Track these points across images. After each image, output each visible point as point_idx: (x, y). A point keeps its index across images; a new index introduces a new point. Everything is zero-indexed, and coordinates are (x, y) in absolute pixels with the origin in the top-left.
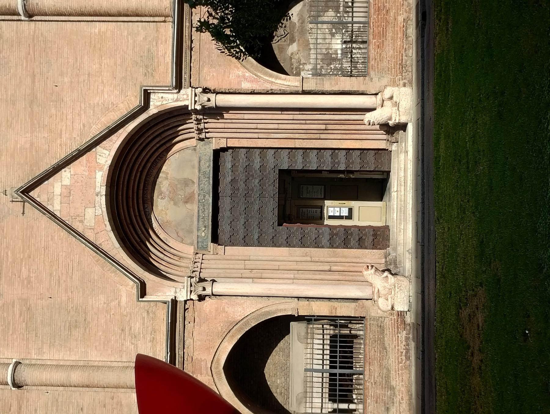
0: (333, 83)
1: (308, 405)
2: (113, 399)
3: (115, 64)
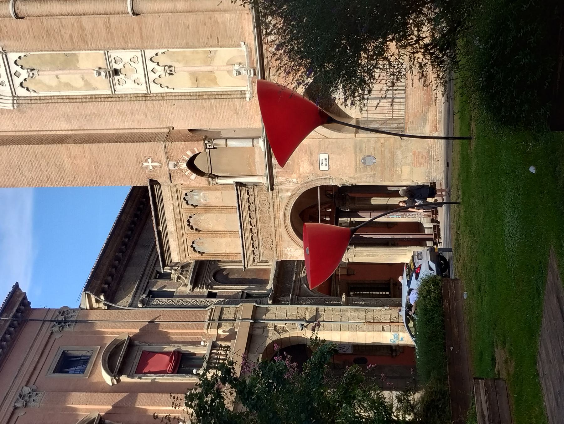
2: (210, 18)
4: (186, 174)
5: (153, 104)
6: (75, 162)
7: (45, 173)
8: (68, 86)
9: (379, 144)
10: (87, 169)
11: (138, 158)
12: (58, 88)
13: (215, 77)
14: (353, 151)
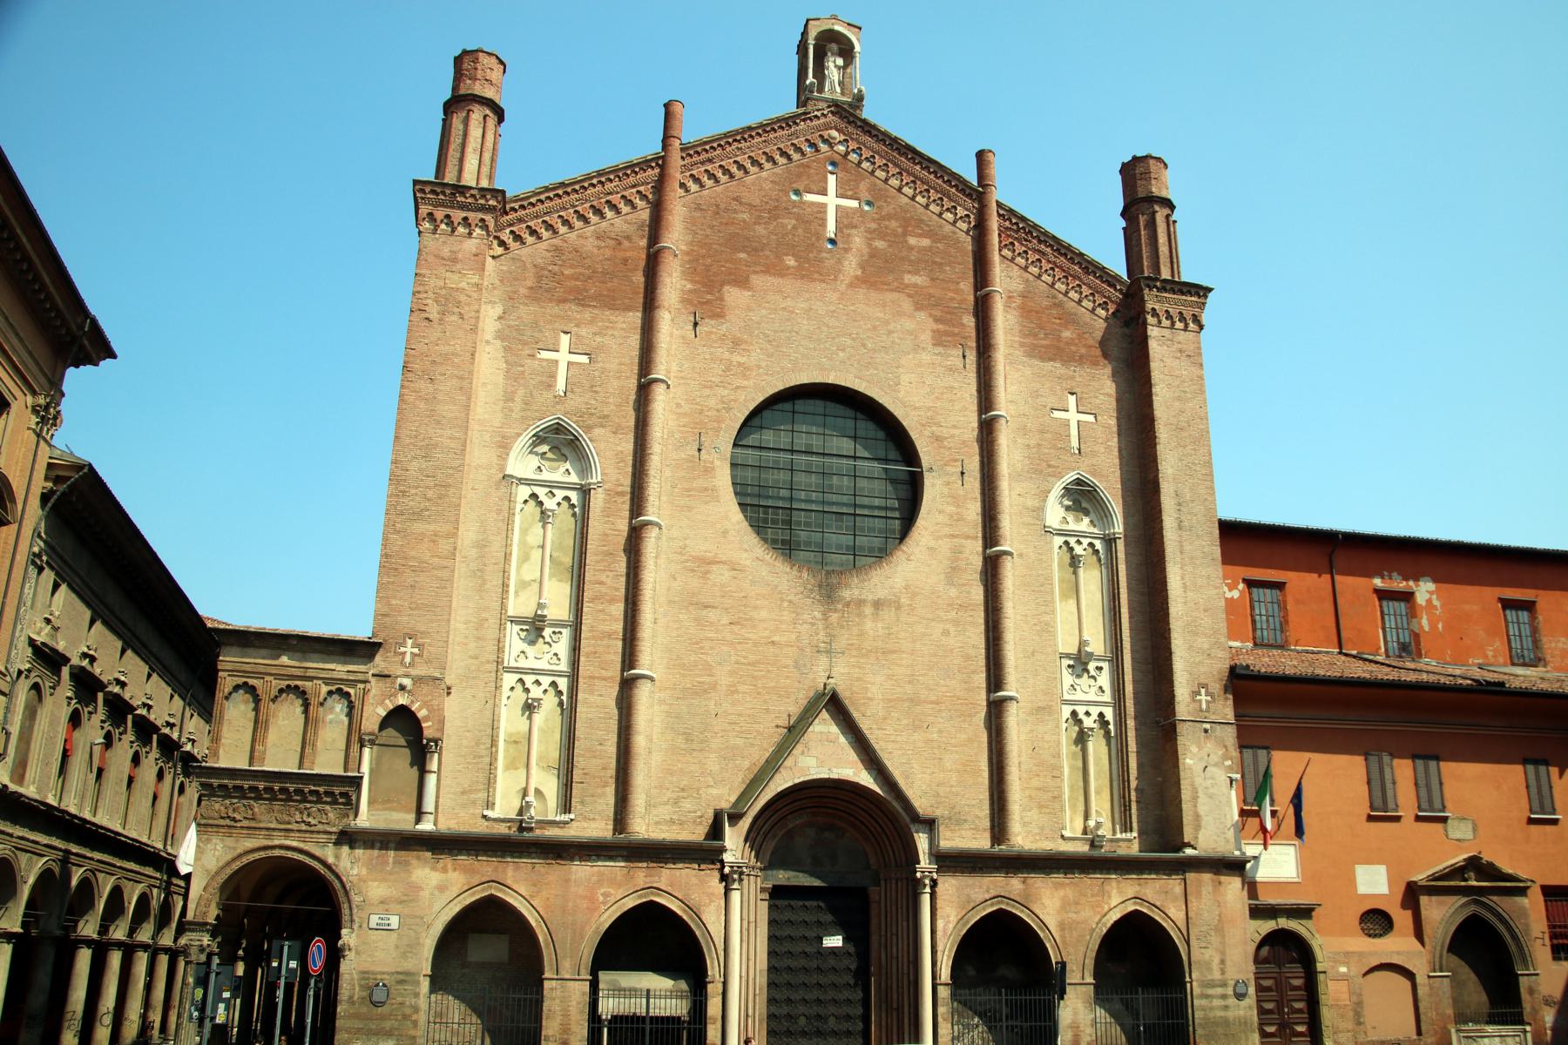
0: (945, 1016)
1: (606, 992)
3: (952, 786)
4: (387, 701)
5: (490, 672)
6: (426, 540)
7: (413, 491)
8: (525, 558)
9: (408, 1011)
10: (413, 553)
11: (421, 633)
12: (523, 543)
13: (517, 769)
14: (399, 970)
